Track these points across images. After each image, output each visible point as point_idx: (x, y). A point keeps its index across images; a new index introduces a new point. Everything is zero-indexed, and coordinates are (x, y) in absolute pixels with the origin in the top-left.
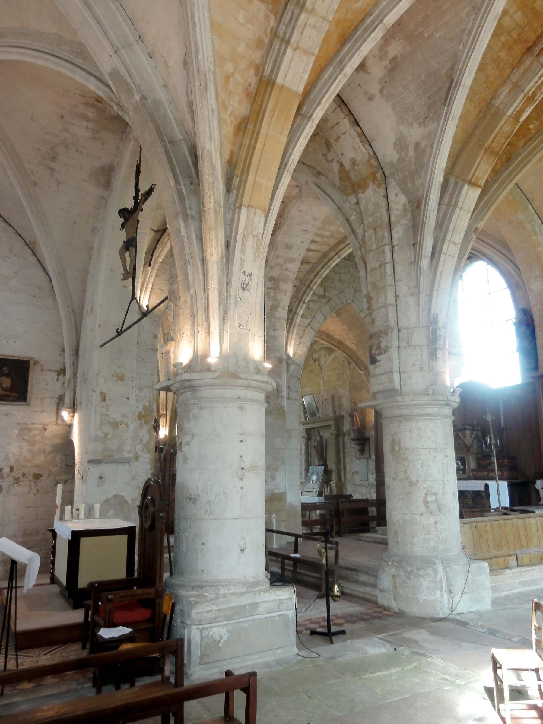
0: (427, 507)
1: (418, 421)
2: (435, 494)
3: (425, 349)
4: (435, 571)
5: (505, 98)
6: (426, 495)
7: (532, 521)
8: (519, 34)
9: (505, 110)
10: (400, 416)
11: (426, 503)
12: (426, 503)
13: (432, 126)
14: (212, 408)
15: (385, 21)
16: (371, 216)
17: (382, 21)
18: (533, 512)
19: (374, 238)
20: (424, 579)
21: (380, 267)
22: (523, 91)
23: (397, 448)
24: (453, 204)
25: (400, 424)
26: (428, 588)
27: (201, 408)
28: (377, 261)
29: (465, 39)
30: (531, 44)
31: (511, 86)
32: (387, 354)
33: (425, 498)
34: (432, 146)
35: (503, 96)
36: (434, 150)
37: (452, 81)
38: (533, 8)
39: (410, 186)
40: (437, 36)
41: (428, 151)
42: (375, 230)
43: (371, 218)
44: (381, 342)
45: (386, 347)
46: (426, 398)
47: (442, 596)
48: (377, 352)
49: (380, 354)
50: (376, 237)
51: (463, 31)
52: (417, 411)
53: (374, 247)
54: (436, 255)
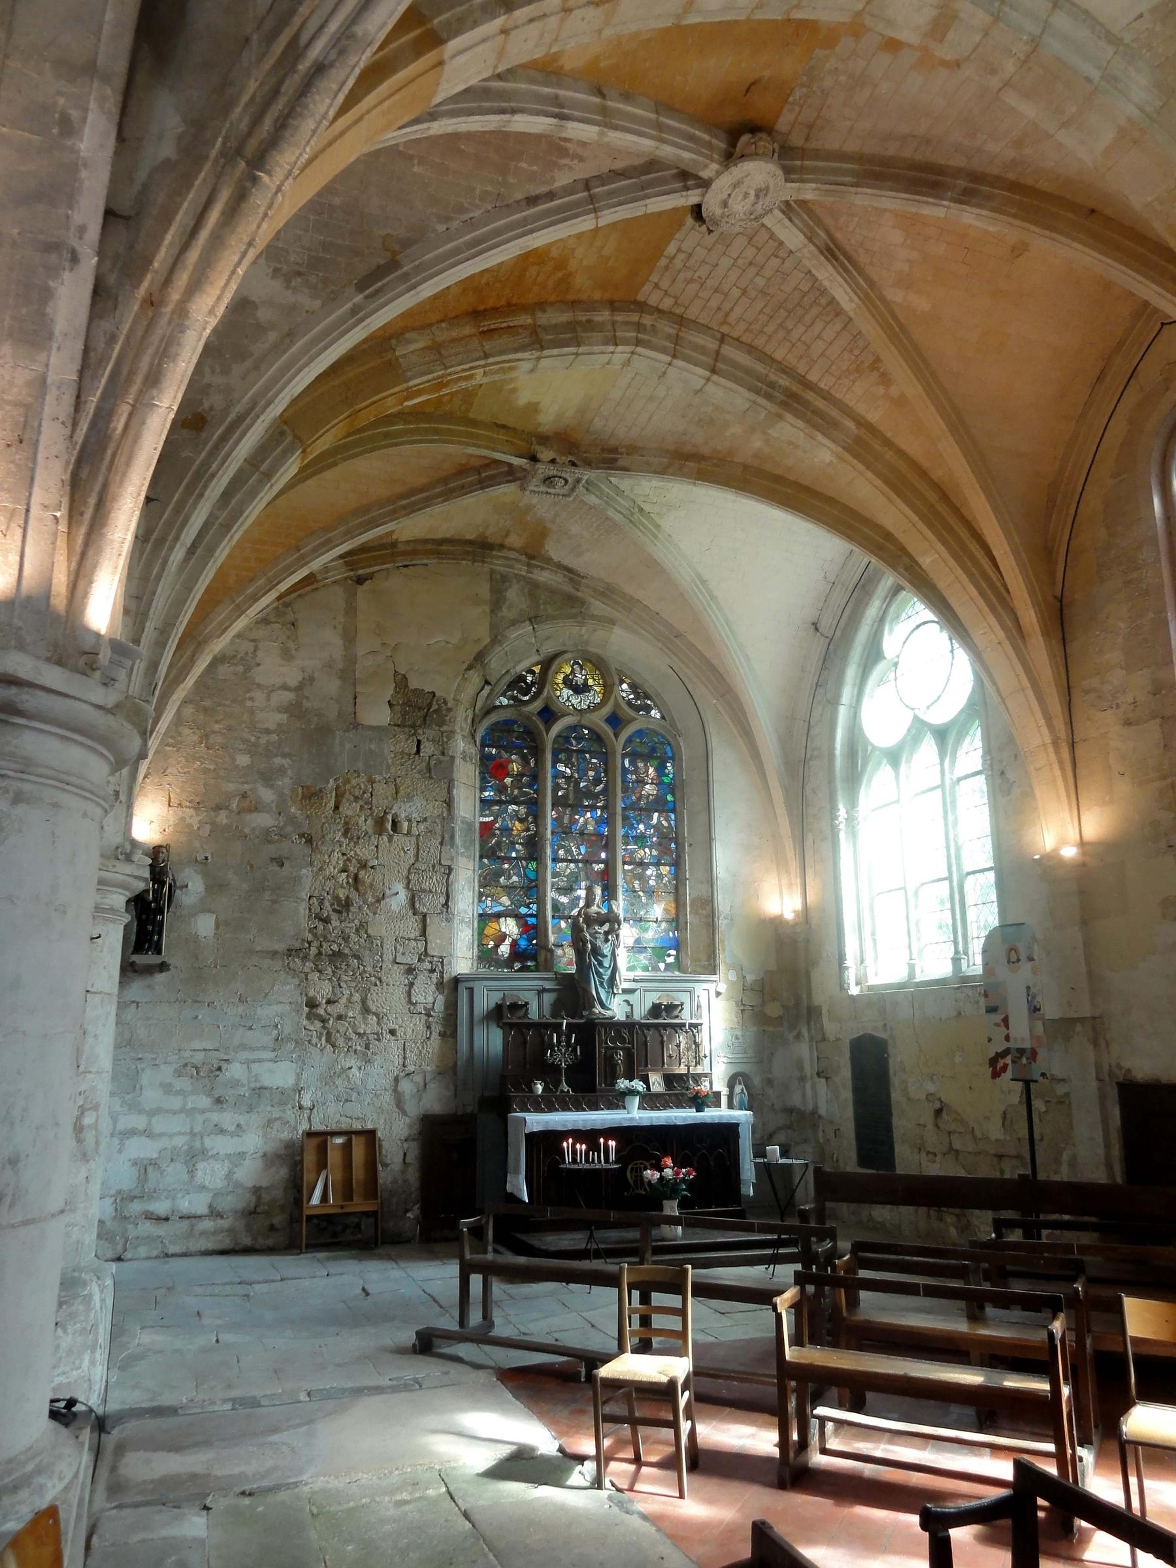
0: (79, 1141)
4: (88, 1299)
5: (412, 352)
6: (82, 1111)
8: (487, 284)
9: (409, 374)
13: (306, 301)
14: (56, 805)
15: (518, 117)
17: (514, 111)
20: (65, 1331)
22: (446, 368)
24: (264, 467)
26: (70, 1352)
27: (18, 798)
29: (455, 224)
30: (481, 308)
31: (430, 343)
33: (79, 1118)
34: (291, 335)
35: (413, 347)
36: (294, 349)
37: (394, 265)
38: (525, 270)
40: (415, 169)
41: (272, 336)
46: (128, 869)
47: (93, 1363)
51: (461, 209)
54: (199, 552)
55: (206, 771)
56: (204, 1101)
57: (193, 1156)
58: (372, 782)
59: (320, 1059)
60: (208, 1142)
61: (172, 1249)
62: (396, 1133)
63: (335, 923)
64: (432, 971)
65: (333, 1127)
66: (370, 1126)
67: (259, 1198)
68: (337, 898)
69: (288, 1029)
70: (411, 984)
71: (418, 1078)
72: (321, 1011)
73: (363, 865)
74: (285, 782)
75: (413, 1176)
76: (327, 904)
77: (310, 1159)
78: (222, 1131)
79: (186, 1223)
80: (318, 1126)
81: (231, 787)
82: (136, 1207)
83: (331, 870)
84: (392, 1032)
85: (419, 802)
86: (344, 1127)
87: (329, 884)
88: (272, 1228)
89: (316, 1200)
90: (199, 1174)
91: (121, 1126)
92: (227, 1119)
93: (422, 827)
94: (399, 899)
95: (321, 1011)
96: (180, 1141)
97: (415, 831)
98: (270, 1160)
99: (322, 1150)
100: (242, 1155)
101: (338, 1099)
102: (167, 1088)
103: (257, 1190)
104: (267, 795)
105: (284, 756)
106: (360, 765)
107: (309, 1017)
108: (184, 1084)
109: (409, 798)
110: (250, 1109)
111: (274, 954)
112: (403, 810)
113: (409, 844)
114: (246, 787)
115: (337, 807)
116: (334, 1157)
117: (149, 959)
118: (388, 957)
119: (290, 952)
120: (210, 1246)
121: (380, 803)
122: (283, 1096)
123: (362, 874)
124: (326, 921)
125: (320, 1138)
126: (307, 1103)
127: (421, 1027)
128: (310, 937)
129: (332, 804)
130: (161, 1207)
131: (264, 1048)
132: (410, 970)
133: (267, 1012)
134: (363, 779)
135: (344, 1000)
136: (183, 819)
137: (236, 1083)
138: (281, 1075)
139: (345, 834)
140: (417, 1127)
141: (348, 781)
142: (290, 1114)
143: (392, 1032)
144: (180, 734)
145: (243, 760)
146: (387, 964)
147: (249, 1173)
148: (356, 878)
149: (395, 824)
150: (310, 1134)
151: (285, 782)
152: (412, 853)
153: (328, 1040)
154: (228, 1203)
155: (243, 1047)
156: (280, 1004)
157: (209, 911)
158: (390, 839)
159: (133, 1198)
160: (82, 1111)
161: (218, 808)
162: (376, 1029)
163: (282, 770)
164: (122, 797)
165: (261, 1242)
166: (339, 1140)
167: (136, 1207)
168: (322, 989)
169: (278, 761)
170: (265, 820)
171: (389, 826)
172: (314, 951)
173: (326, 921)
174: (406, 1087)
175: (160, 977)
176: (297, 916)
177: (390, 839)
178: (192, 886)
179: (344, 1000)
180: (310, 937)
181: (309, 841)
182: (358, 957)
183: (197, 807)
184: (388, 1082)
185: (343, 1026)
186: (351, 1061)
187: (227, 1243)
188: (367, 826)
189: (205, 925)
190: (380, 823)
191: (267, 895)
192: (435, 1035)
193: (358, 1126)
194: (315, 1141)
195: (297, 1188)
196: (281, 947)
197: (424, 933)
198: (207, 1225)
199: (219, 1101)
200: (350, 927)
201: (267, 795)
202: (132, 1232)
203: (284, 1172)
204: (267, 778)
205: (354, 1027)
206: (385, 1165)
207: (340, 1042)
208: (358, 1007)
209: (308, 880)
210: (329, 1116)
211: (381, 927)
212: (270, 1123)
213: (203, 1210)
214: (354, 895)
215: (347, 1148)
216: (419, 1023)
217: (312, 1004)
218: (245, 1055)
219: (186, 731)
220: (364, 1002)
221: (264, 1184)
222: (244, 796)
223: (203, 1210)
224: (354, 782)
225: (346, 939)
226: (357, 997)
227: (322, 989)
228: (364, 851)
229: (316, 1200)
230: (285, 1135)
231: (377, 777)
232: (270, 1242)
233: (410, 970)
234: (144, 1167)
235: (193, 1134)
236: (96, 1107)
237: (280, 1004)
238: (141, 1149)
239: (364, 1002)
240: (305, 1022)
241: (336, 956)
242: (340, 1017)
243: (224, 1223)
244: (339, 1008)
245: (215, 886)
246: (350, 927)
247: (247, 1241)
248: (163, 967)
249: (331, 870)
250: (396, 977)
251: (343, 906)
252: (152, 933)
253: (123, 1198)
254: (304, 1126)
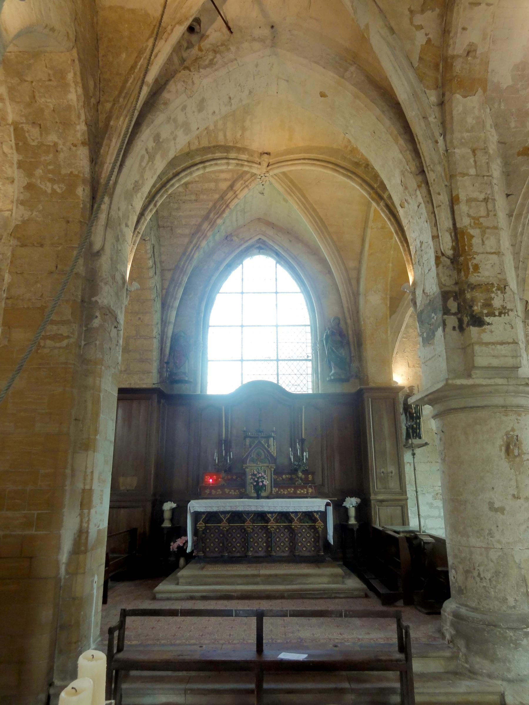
10: (518, 406)
16: (468, 131)
19: (472, 160)
21: (486, 200)
23: (516, 452)
25: (519, 418)
28: (481, 192)
32: (504, 319)
39: (513, 125)
42: (474, 151)
43: (468, 134)
44: (492, 299)
45: (504, 308)
48: (485, 311)
49: (491, 314)
50: (475, 161)
53: (472, 171)
117: (416, 441)
136: (416, 373)
144: (408, 332)
219: (411, 331)
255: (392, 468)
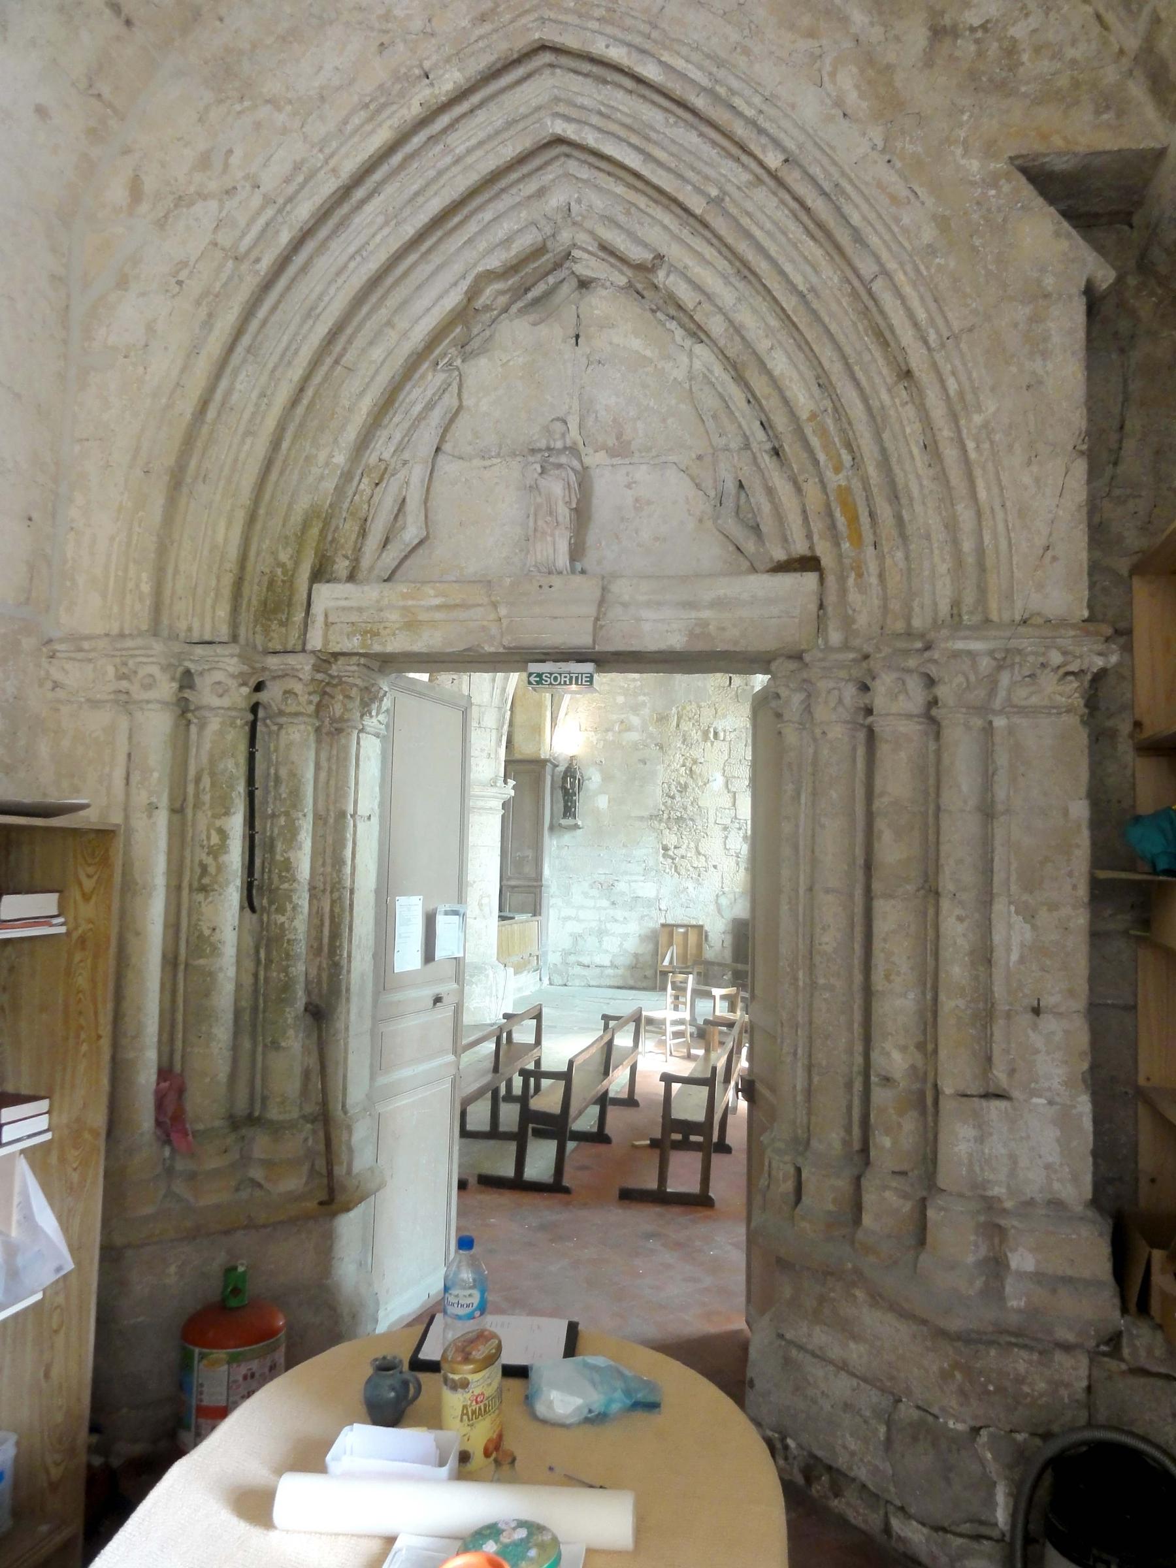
1: (480, 814)
2: (489, 896)
3: (494, 732)
4: (487, 976)
6: (482, 897)
7: (516, 927)
11: (480, 905)
12: (480, 905)
18: (513, 918)
46: (494, 790)
52: (480, 803)
55: (599, 708)
56: (605, 903)
57: (601, 933)
58: (700, 707)
59: (670, 882)
60: (608, 926)
61: (592, 983)
62: (717, 929)
63: (678, 798)
64: (740, 829)
65: (680, 922)
66: (701, 923)
67: (637, 959)
68: (679, 783)
69: (651, 863)
70: (726, 837)
71: (731, 896)
72: (670, 853)
73: (695, 762)
74: (646, 712)
75: (728, 955)
76: (673, 787)
77: (663, 940)
78: (616, 921)
79: (598, 970)
80: (670, 921)
81: (614, 717)
82: (572, 959)
83: (675, 766)
84: (715, 867)
85: (730, 718)
86: (685, 922)
87: (674, 775)
88: (645, 977)
89: (666, 962)
90: (605, 943)
91: (563, 914)
92: (619, 914)
93: (733, 735)
94: (718, 782)
95: (670, 853)
96: (594, 924)
97: (728, 738)
98: (643, 939)
99: (671, 935)
100: (627, 935)
101: (682, 906)
102: (586, 895)
103: (636, 955)
104: (635, 720)
105: (644, 695)
106: (692, 698)
107: (664, 856)
108: (594, 892)
109: (724, 716)
110: (631, 909)
111: (641, 818)
112: (720, 725)
113: (725, 747)
114: (623, 716)
115: (678, 725)
116: (677, 939)
118: (711, 820)
119: (651, 817)
120: (612, 983)
121: (705, 722)
122: (649, 903)
123: (694, 767)
124: (673, 798)
125: (669, 928)
126: (663, 907)
127: (733, 864)
128: (663, 808)
129: (675, 723)
130: (586, 960)
131: (638, 874)
132: (725, 828)
133: (639, 853)
134: (694, 706)
135: (684, 847)
137: (623, 894)
138: (647, 890)
139: (683, 743)
140: (730, 927)
141: (684, 708)
142: (654, 913)
143: (715, 867)
145: (621, 699)
146: (711, 824)
147: (632, 945)
148: (691, 770)
149: (716, 734)
150: (663, 925)
151: (646, 712)
152: (726, 753)
153: (676, 870)
154: (621, 961)
155: (626, 873)
156: (646, 849)
157: (605, 793)
158: (712, 743)
159: (571, 954)
160: (482, 897)
161: (607, 730)
162: (705, 864)
163: (644, 704)
164: (492, 756)
165: (639, 984)
166: (682, 930)
167: (572, 959)
168: (671, 839)
169: (641, 698)
170: (634, 736)
171: (711, 735)
172: (665, 816)
173: (673, 798)
174: (724, 901)
175: (579, 832)
176: (655, 795)
177: (712, 743)
178: (594, 779)
179: (684, 847)
180: (663, 808)
181: (661, 748)
182: (692, 820)
183: (596, 730)
184: (713, 898)
185: (685, 862)
186: (690, 885)
187: (620, 983)
188: (696, 735)
189: (602, 802)
190: (706, 734)
191: (637, 783)
192: (742, 870)
193: (694, 923)
194: (667, 929)
195: (656, 954)
196: (646, 814)
197: (734, 805)
198: (610, 971)
199: (613, 903)
200: (688, 801)
201: (635, 720)
202: (571, 972)
203: (651, 947)
204: (635, 709)
205: (691, 863)
206: (711, 947)
207: (683, 872)
208: (694, 851)
209: (661, 773)
210: (677, 915)
211: (706, 801)
212: (642, 917)
213: (607, 963)
214: (690, 782)
215: (686, 934)
216: (732, 862)
217: (666, 848)
218: (627, 878)
220: (697, 848)
221: (640, 951)
222: (622, 722)
223: (607, 963)
224: (688, 708)
225: (685, 809)
226: (692, 845)
227: (671, 839)
228: (696, 753)
229: (666, 962)
230: (652, 925)
231: (703, 704)
232: (644, 985)
233: (725, 828)
234: (576, 938)
235: (600, 921)
236: (489, 896)
237: (646, 849)
238: (573, 927)
239: (697, 848)
240: (661, 859)
241: (679, 819)
242: (683, 857)
243: (620, 972)
244: (682, 851)
245: (607, 778)
246: (688, 801)
247: (631, 983)
248: (576, 827)
249: (675, 766)
250: (716, 833)
251: (683, 788)
252: (570, 808)
253: (567, 953)
254: (662, 921)
255: (530, 853)
